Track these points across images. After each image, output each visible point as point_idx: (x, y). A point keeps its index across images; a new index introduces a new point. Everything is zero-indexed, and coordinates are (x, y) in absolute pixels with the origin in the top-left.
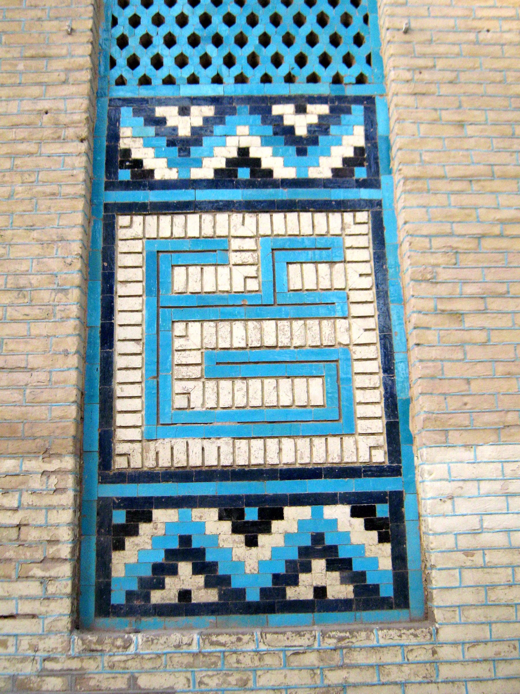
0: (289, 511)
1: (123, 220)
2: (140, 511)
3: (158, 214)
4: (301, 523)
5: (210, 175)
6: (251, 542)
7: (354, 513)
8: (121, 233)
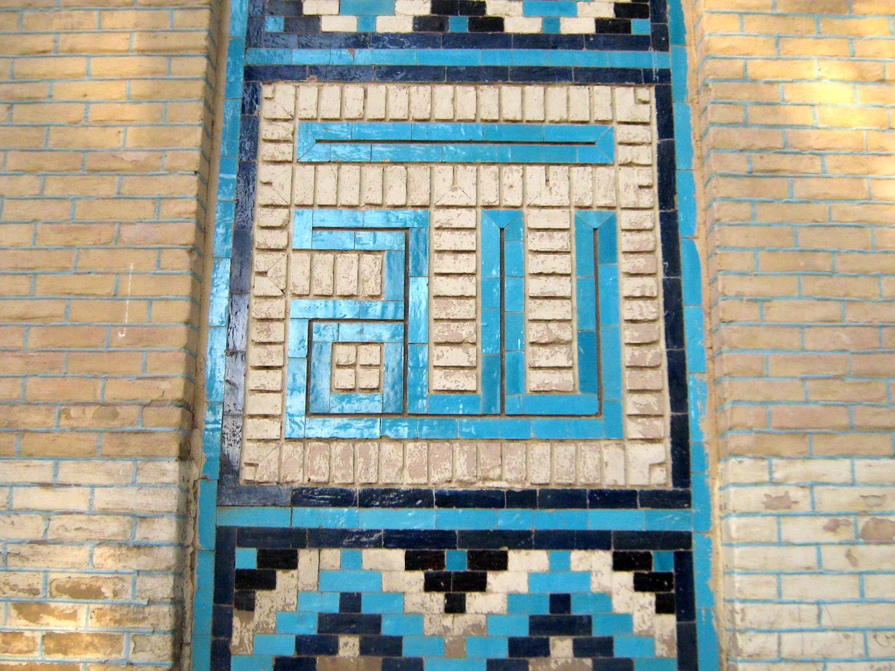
0: (516, 558)
2: (280, 552)
4: (533, 577)
5: (407, 27)
6: (455, 606)
7: (619, 564)
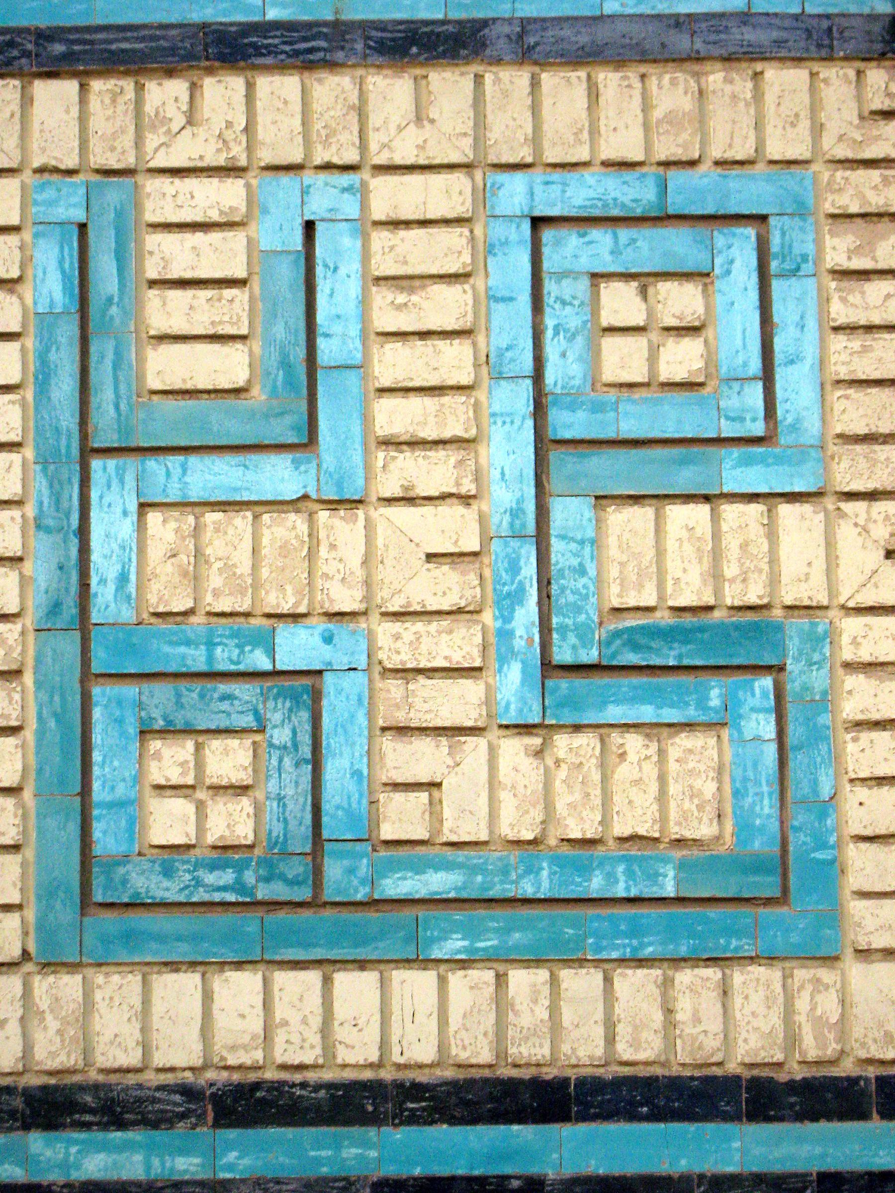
3: (83, 77)
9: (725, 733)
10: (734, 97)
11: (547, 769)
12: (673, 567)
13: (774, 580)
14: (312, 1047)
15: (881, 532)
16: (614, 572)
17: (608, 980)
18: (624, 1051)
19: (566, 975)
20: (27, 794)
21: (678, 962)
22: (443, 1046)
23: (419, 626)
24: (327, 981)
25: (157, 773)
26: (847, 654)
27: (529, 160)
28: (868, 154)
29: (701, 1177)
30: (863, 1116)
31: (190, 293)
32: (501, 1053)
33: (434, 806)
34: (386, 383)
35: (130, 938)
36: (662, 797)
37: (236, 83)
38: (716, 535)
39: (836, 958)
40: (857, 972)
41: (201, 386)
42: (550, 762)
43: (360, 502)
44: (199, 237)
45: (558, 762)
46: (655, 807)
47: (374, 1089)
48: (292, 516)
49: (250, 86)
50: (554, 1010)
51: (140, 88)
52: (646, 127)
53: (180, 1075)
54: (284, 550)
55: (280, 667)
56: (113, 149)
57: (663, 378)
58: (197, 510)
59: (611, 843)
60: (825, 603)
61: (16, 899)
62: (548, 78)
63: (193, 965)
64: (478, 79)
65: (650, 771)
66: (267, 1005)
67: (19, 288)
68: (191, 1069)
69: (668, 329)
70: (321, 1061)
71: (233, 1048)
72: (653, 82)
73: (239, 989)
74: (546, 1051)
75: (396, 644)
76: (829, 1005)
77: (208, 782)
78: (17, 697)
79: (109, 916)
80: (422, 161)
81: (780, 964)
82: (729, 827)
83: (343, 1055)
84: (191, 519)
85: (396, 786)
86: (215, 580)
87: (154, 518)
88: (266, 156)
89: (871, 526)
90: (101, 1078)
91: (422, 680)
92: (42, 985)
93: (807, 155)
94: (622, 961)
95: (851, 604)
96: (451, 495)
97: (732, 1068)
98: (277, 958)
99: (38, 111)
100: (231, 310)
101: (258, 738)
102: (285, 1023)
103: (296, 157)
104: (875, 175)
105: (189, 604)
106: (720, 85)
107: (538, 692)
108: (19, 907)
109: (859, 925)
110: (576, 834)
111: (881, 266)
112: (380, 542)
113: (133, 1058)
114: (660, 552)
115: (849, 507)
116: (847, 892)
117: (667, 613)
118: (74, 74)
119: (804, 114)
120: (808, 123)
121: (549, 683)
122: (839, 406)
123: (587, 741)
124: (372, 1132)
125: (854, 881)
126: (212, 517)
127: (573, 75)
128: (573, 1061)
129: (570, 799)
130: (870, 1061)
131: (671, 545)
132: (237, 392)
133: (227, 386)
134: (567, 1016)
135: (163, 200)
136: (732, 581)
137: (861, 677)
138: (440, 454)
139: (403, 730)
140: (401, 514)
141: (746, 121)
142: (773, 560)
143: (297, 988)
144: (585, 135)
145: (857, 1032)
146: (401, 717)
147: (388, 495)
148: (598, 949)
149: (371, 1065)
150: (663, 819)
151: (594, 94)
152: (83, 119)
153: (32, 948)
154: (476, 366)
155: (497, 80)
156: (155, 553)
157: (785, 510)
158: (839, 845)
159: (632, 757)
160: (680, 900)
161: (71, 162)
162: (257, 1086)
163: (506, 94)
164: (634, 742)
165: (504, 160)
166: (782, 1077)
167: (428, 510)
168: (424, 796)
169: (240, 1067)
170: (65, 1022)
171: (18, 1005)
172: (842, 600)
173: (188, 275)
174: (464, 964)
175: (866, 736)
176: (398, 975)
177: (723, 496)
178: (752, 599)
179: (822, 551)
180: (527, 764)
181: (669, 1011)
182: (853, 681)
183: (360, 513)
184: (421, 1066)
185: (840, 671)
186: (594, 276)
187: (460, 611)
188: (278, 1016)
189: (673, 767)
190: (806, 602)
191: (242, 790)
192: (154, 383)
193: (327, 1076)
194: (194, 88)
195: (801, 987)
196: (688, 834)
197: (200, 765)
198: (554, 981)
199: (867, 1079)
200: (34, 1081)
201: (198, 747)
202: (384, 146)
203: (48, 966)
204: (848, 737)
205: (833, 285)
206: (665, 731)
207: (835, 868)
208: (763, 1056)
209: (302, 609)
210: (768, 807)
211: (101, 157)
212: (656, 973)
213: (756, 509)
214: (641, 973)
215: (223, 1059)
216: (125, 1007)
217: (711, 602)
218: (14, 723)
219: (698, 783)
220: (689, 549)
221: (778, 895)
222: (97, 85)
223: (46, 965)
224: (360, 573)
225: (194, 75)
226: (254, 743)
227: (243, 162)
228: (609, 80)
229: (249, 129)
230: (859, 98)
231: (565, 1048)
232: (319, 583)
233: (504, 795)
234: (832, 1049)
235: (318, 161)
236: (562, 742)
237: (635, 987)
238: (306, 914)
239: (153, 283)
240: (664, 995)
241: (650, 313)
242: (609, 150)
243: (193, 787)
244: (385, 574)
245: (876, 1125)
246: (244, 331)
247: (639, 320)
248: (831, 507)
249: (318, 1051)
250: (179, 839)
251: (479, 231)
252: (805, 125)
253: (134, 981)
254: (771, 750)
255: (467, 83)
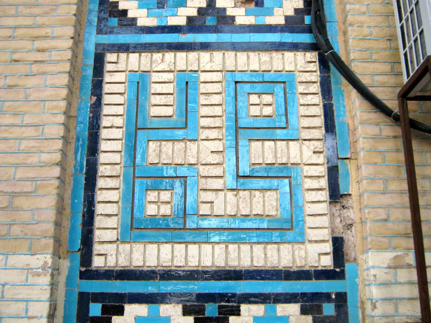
1: (110, 57)
3: (140, 53)
8: (108, 67)
9: (278, 191)
10: (278, 58)
11: (237, 199)
12: (266, 154)
13: (289, 158)
14: (183, 262)
15: (312, 148)
16: (253, 155)
17: (251, 247)
18: (255, 264)
19: (242, 246)
20: (120, 203)
21: (267, 243)
22: (213, 262)
23: (209, 167)
24: (186, 247)
25: (149, 199)
26: (305, 174)
27: (234, 70)
28: (307, 70)
29: (273, 293)
30: (311, 279)
31: (161, 96)
32: (227, 264)
33: (212, 207)
34: (203, 115)
35: (143, 236)
36: (264, 205)
37: (172, 54)
38: (276, 148)
39: (304, 243)
40: (309, 246)
41: (162, 115)
42: (238, 197)
43: (196, 140)
44: (163, 85)
45: (240, 197)
46: (262, 208)
47: (197, 272)
48: (181, 143)
49: (175, 55)
50: (239, 254)
51: (152, 55)
52: (259, 63)
53: (152, 268)
54: (179, 150)
55: (177, 176)
56: (145, 67)
57: (263, 115)
58: (161, 142)
59: (252, 216)
60: (300, 163)
61: (116, 227)
62: (239, 54)
63: (156, 242)
64: (224, 54)
65: (261, 200)
66: (172, 252)
67: (124, 95)
68: (155, 267)
69: (264, 105)
70: (185, 265)
71: (164, 262)
72: (261, 55)
73: (166, 248)
74: (237, 264)
75: (204, 171)
76: (303, 253)
77: (161, 201)
78: (118, 181)
79: (138, 231)
80: (212, 70)
81: (291, 244)
82: (279, 213)
83: (190, 264)
84: (159, 143)
85: (203, 202)
86: (164, 156)
87: (151, 143)
88: (178, 68)
89: (310, 146)
90: (134, 268)
91: (209, 179)
92: (121, 246)
93: (294, 70)
94: (255, 243)
95: (306, 163)
96: (217, 139)
97: (280, 268)
98: (175, 241)
99: (130, 60)
100: (170, 100)
101: (172, 191)
102: (177, 256)
103: (184, 68)
104: (308, 74)
105: (158, 161)
106: (275, 55)
107: (235, 182)
108: (117, 228)
109: (309, 235)
110: (244, 214)
111: (311, 92)
112: (201, 148)
113: (141, 264)
114: (263, 152)
115: (304, 142)
116: (306, 228)
117: (265, 165)
118: (138, 52)
119: (293, 61)
120: (294, 64)
121: (238, 180)
122: (302, 121)
123: (247, 193)
124: (196, 282)
125: (308, 224)
126: (164, 143)
127: (244, 53)
128: (244, 266)
129: (243, 206)
130: (312, 266)
131: (265, 150)
132: (170, 117)
133: (168, 115)
134: (242, 255)
135: (155, 77)
136: (279, 158)
137: (308, 179)
138: (215, 130)
139: (205, 190)
140: (205, 142)
141: (281, 62)
142: (288, 154)
143: (180, 248)
144: (247, 65)
145: (309, 260)
146: (204, 187)
147: (203, 138)
148: (249, 240)
149: (196, 266)
150: (264, 210)
151: (248, 57)
152: (140, 61)
153: (119, 238)
154: (223, 112)
155: (228, 54)
156: (151, 150)
157: (291, 143)
158: (304, 217)
159: (257, 196)
160: (268, 229)
161: (136, 69)
162: (169, 271)
163: (230, 57)
164: (257, 193)
165: (229, 70)
166: (292, 270)
167: (211, 142)
168: (210, 205)
169: (166, 266)
170: (126, 255)
171: (115, 251)
172: (304, 162)
173: (161, 92)
174: (218, 243)
175: (310, 192)
176: (203, 245)
177: (277, 140)
178: (284, 162)
179: (299, 152)
180: (233, 198)
181: (265, 255)
182: (306, 180)
183: (196, 142)
184: (208, 267)
185: (304, 178)
186: (248, 93)
187: (218, 164)
188: (175, 255)
189: (266, 199)
190: (296, 163)
191: (169, 203)
192: (152, 114)
193: (186, 269)
194: (163, 55)
195: (296, 249)
196: (270, 214)
197: (159, 197)
198: (239, 248)
199: (312, 271)
200: (118, 269)
201: (159, 193)
202: (204, 67)
203: (122, 242)
204: (306, 192)
205: (300, 96)
206: (264, 191)
207: (304, 221)
208: (287, 265)
209: (183, 163)
210: (288, 207)
211: (143, 68)
212: (262, 246)
213: (284, 142)
214: (259, 245)
215: (162, 264)
216: (140, 252)
217: (275, 162)
218: (117, 187)
219: (272, 202)
220: (270, 151)
221: (290, 228)
222: (143, 54)
223: (122, 242)
224: (196, 155)
225: (164, 53)
226: (171, 192)
227: (173, 70)
228: (252, 54)
229: (174, 63)
230: (304, 59)
231: (242, 263)
232: (187, 157)
233: (228, 205)
234: (303, 264)
235: (189, 70)
236: (241, 193)
237: (258, 249)
238: (182, 231)
239: (153, 94)
240: (264, 251)
241: (261, 101)
242: (252, 68)
243: (157, 202)
244: (202, 156)
245: (314, 281)
246: (172, 104)
247: (258, 103)
248: (301, 142)
249: (184, 263)
250: (153, 214)
251: (223, 84)
252: (293, 64)
253: (142, 246)
254: (289, 195)
255: (221, 54)
